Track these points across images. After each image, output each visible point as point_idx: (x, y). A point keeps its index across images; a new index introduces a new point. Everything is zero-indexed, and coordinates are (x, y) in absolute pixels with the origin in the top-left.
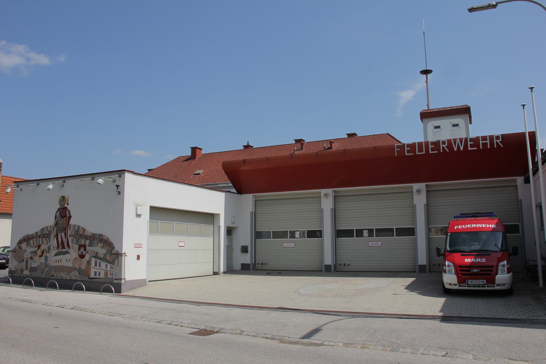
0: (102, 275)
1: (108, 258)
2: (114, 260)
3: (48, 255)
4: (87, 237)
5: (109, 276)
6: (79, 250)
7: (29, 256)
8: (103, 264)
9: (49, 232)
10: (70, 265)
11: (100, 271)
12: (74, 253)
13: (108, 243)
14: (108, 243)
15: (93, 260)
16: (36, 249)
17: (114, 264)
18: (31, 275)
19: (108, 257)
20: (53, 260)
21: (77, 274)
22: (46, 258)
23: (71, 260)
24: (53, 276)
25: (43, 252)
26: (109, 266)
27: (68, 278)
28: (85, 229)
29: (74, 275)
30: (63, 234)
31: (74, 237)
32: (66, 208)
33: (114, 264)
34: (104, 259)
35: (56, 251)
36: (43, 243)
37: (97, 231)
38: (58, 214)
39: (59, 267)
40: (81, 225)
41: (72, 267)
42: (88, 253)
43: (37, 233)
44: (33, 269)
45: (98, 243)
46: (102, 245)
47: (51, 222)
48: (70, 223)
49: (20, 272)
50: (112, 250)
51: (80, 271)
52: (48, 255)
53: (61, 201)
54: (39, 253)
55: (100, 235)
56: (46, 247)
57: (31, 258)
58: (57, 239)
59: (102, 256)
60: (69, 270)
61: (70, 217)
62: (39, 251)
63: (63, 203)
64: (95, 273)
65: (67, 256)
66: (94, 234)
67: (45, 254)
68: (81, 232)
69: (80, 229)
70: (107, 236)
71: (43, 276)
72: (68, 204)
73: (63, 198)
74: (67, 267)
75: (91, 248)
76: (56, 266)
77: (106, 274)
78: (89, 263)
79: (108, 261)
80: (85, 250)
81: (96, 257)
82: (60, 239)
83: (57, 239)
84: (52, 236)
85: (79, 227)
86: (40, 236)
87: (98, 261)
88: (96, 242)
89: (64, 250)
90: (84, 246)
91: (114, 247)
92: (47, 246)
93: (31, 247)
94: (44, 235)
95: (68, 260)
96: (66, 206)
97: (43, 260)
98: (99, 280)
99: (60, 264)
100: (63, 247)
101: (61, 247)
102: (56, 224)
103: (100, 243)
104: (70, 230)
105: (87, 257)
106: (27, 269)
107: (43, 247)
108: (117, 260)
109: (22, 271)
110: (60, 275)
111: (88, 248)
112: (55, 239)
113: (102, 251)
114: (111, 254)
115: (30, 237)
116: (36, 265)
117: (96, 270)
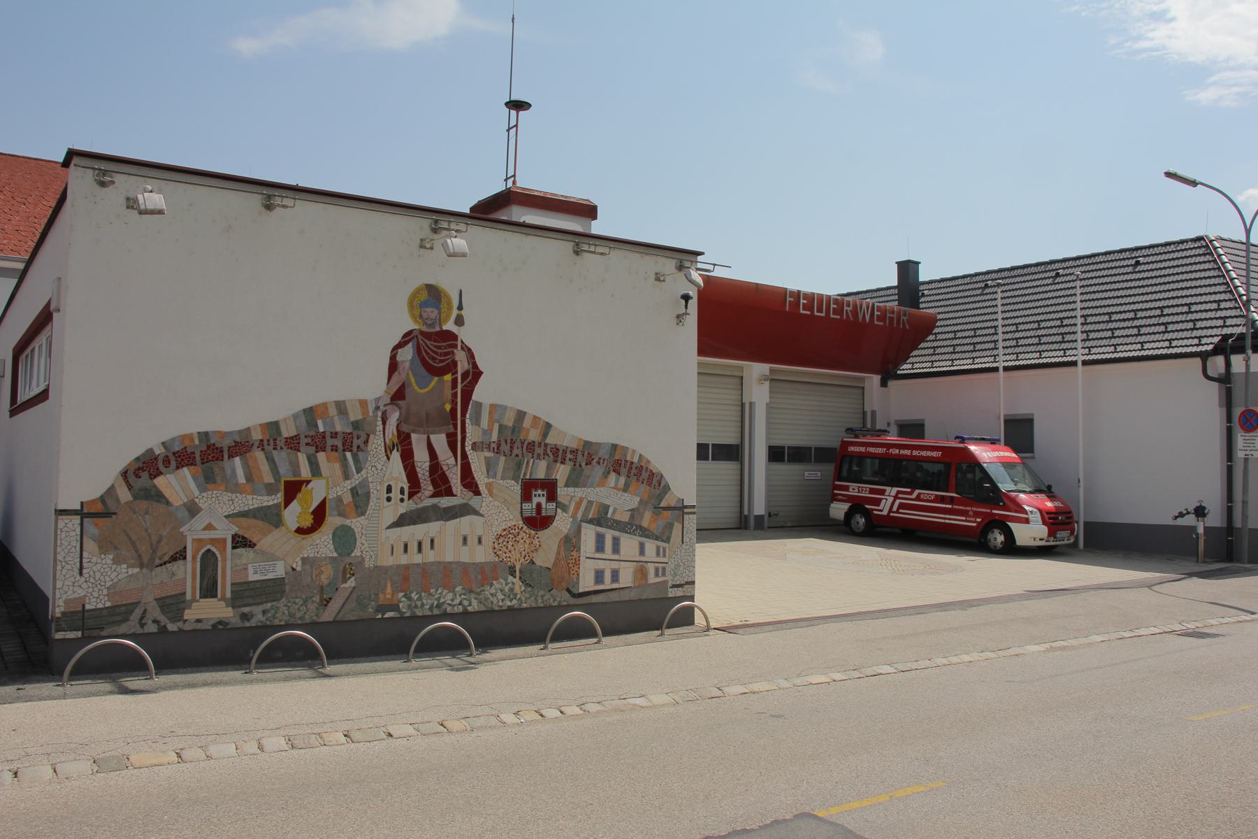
0: (626, 579)
1: (645, 524)
2: (670, 526)
3: (356, 523)
4: (558, 455)
5: (652, 579)
6: (526, 497)
7: (226, 531)
8: (629, 544)
9: (356, 425)
10: (482, 555)
11: (615, 565)
12: (499, 507)
13: (645, 475)
14: (645, 475)
15: (589, 535)
16: (279, 498)
17: (668, 540)
18: (245, 617)
19: (646, 520)
20: (382, 540)
21: (518, 586)
22: (345, 539)
23: (488, 540)
24: (395, 607)
25: (319, 514)
26: (651, 546)
27: (475, 606)
28: (548, 426)
29: (504, 594)
30: (440, 441)
31: (498, 451)
32: (451, 336)
33: (668, 540)
34: (632, 526)
35: (402, 509)
36: (316, 470)
37: (601, 434)
38: (406, 354)
39: (424, 569)
40: (531, 410)
41: (494, 566)
42: (564, 508)
43: (274, 427)
44: (245, 593)
45: (606, 475)
46: (622, 480)
47: (360, 378)
48: (476, 396)
49: (155, 612)
50: (660, 497)
51: (530, 575)
52: (356, 523)
53: (423, 305)
54: (295, 514)
55: (614, 447)
56: (343, 490)
57: (241, 542)
58: (407, 456)
59: (625, 517)
60: (486, 573)
61: (475, 374)
62: (294, 505)
63: (431, 313)
64: (599, 576)
65: (465, 524)
66: (587, 444)
67: (332, 521)
68: (534, 435)
69: (527, 423)
70: (639, 451)
71: (328, 615)
72: (460, 321)
73: (433, 295)
74: (465, 567)
75: (579, 492)
76: (407, 567)
77: (641, 572)
78: (571, 543)
79: (645, 533)
80: (552, 497)
81: (601, 519)
82: (421, 458)
83: (407, 456)
84: (377, 444)
85: (521, 415)
86: (293, 444)
87: (609, 535)
88: (598, 471)
89: (445, 502)
90: (550, 488)
91: (667, 488)
92: (348, 484)
93: (235, 488)
94: (324, 435)
95: (472, 540)
96: (450, 326)
97: (322, 544)
98: (614, 597)
99: (430, 556)
100: (437, 489)
101: (427, 488)
102: (399, 395)
103: (613, 476)
104: (477, 421)
105: (562, 523)
106: (209, 590)
107: (317, 491)
108: (677, 526)
109: (173, 605)
110: (428, 602)
111: (563, 492)
112: (396, 455)
113: (621, 502)
114: (658, 509)
115: (227, 443)
116: (279, 571)
117: (601, 565)
